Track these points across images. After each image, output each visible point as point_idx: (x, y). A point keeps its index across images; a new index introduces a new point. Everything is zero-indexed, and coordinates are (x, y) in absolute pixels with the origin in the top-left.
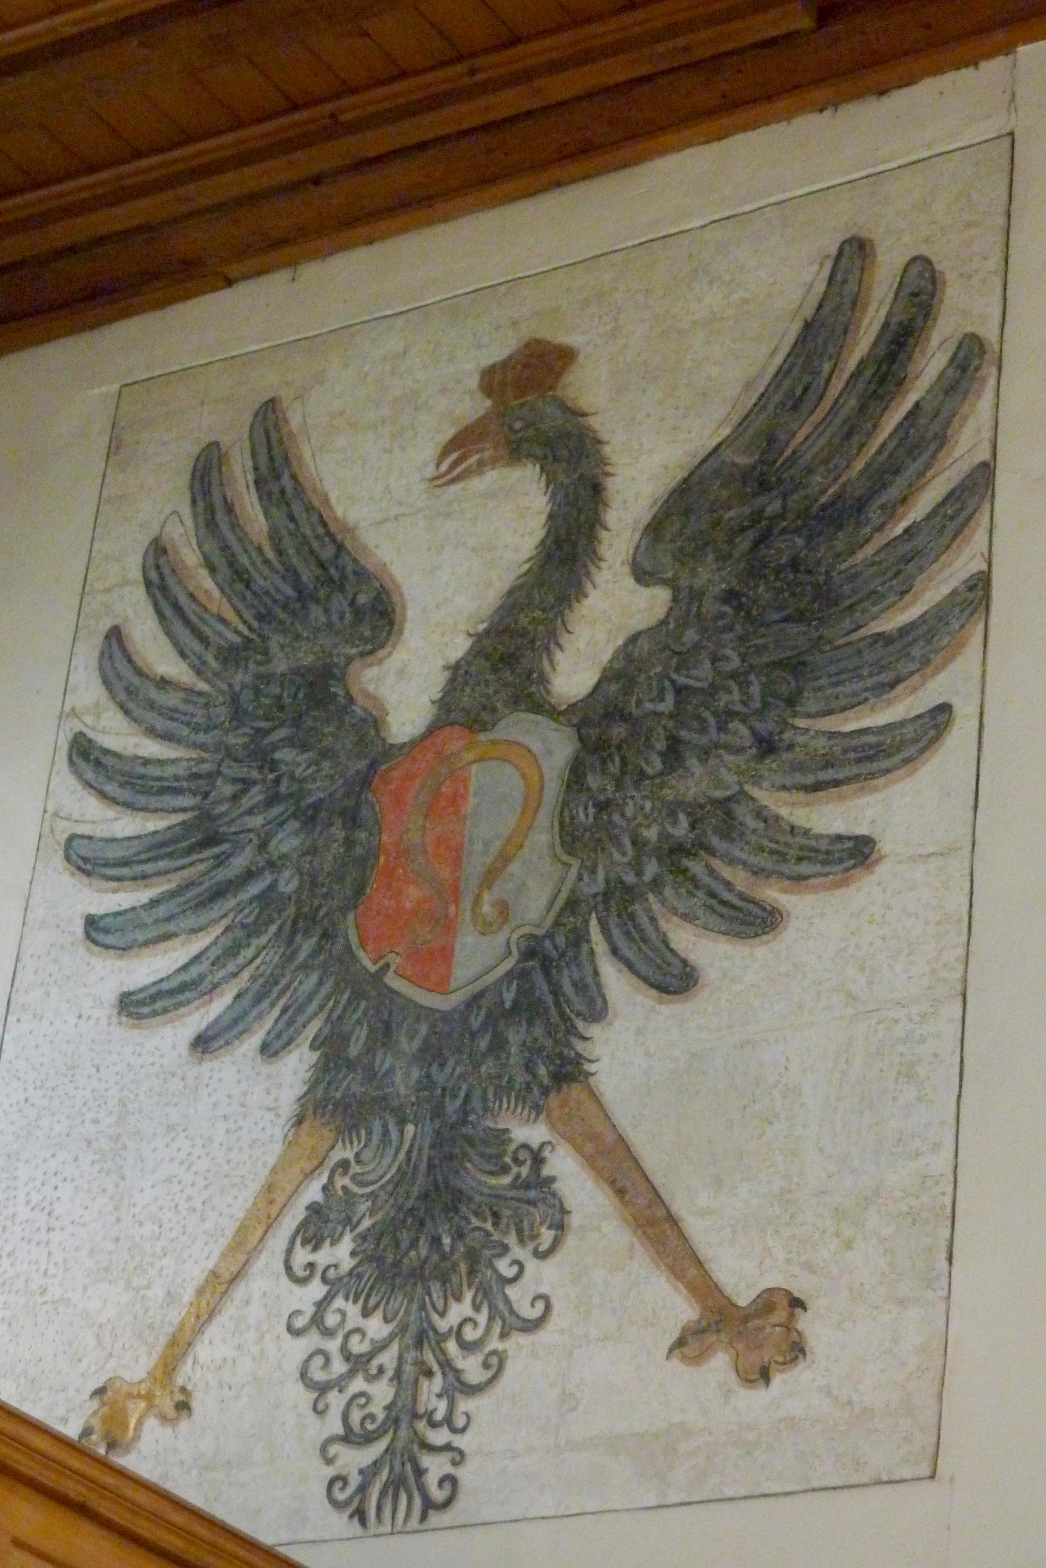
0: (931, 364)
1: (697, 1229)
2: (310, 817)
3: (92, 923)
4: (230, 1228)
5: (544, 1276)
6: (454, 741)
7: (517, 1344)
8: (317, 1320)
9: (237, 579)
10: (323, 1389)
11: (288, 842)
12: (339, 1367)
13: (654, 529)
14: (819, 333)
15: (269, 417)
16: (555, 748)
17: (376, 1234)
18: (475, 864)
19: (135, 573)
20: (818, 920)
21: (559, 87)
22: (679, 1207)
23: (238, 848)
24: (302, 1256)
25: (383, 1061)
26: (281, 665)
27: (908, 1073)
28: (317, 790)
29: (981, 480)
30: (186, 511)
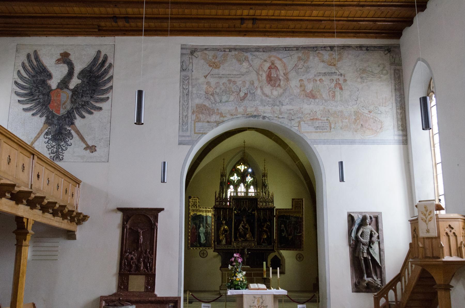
0: (107, 65)
1: (86, 139)
2: (43, 95)
3: (19, 101)
4: (38, 133)
5: (70, 142)
6: (59, 90)
7: (68, 147)
8: (48, 142)
9: (33, 68)
10: (49, 149)
11: (41, 96)
12: (50, 147)
13: (80, 74)
15: (35, 52)
16: (70, 93)
17: (54, 135)
18: (62, 102)
19: (21, 65)
20: (96, 114)
21: (71, 30)
22: (84, 137)
23: (35, 96)
24: (46, 136)
27: (105, 129)
28: (44, 92)
29: (112, 77)
30: (26, 59)
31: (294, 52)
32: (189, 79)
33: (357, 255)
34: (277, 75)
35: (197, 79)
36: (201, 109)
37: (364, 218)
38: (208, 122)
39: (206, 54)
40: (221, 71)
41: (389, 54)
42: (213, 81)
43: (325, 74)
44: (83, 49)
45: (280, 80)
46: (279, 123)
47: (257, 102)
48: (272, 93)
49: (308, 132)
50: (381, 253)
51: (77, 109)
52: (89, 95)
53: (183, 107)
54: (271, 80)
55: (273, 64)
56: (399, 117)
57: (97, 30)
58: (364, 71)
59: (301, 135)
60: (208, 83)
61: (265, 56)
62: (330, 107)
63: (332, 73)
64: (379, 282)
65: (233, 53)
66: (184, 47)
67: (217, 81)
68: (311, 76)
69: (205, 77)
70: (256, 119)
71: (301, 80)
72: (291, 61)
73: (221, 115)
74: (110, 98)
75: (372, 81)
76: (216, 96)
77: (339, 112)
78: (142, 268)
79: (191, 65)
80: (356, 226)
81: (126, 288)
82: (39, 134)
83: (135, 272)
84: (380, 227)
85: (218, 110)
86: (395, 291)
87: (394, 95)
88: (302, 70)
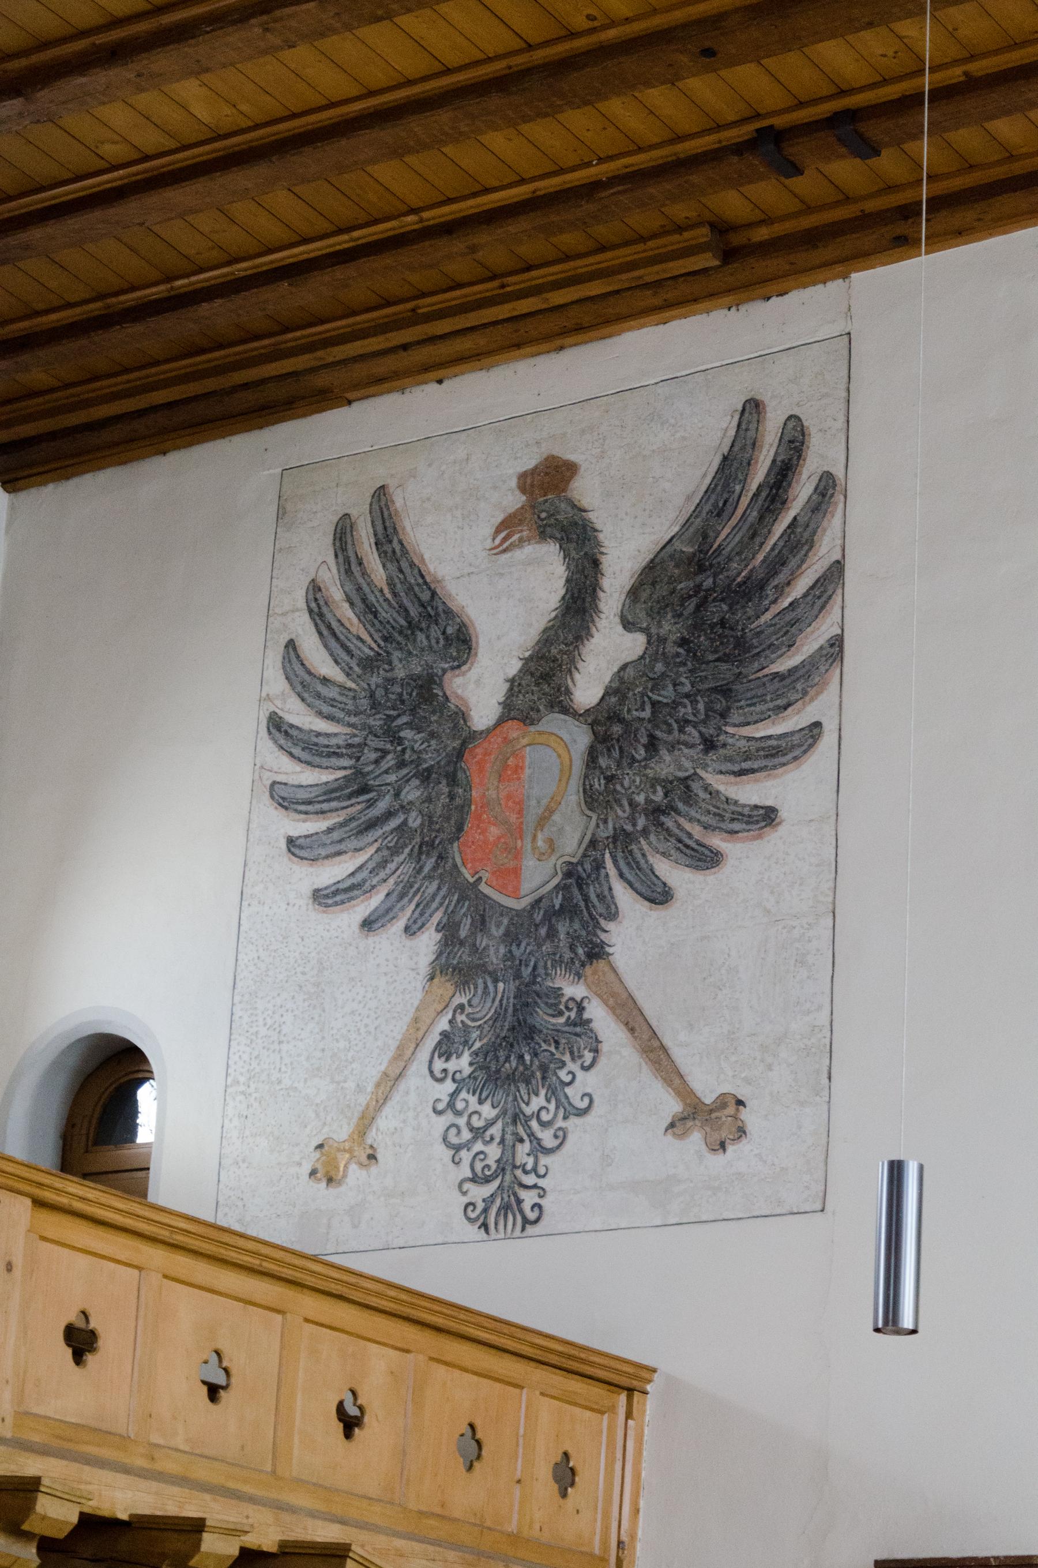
0: (802, 491)
1: (678, 1054)
2: (426, 777)
3: (291, 841)
4: (393, 1045)
5: (586, 1082)
6: (513, 730)
7: (573, 1123)
8: (451, 1105)
9: (369, 611)
10: (457, 1148)
11: (412, 793)
12: (466, 1135)
13: (633, 593)
14: (732, 465)
18: (533, 812)
19: (302, 604)
21: (558, 297)
22: (667, 1041)
24: (439, 1065)
25: (482, 942)
26: (400, 673)
27: (801, 962)
28: (430, 760)
29: (836, 571)
52: (693, 734)
82: (399, 1055)
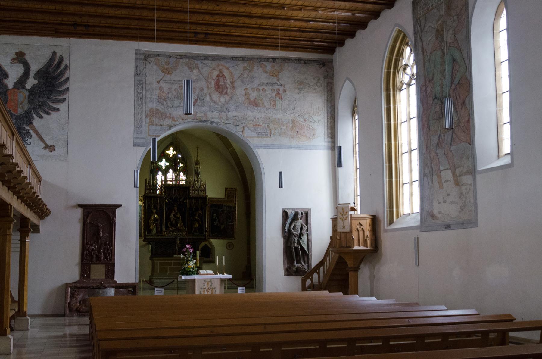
0: (63, 66)
1: (44, 139)
6: (15, 90)
14: (52, 59)
16: (27, 94)
20: (54, 115)
27: (63, 129)
29: (68, 79)
31: (240, 62)
32: (142, 84)
33: (289, 245)
34: (225, 83)
35: (150, 84)
36: (154, 113)
37: (296, 214)
38: (161, 125)
39: (159, 59)
40: (173, 77)
41: (323, 68)
42: (165, 87)
43: (267, 84)
44: (40, 49)
45: (227, 88)
46: (225, 128)
47: (206, 108)
48: (219, 99)
49: (251, 137)
50: (309, 243)
51: (35, 109)
53: (138, 111)
54: (219, 88)
55: (221, 72)
56: (329, 125)
57: (54, 32)
58: (301, 83)
59: (245, 140)
60: (161, 88)
61: (214, 64)
62: (270, 115)
63: (273, 83)
64: (306, 267)
65: (184, 60)
66: (138, 52)
67: (170, 87)
68: (255, 85)
69: (158, 82)
70: (205, 124)
71: (246, 89)
72: (237, 70)
73: (173, 119)
74: (67, 99)
75: (308, 92)
76: (168, 101)
77: (279, 119)
78: (102, 258)
79: (145, 70)
80: (289, 220)
81: (89, 276)
83: (96, 261)
84: (309, 221)
85: (170, 114)
86: (318, 274)
87: (326, 106)
88: (247, 80)
